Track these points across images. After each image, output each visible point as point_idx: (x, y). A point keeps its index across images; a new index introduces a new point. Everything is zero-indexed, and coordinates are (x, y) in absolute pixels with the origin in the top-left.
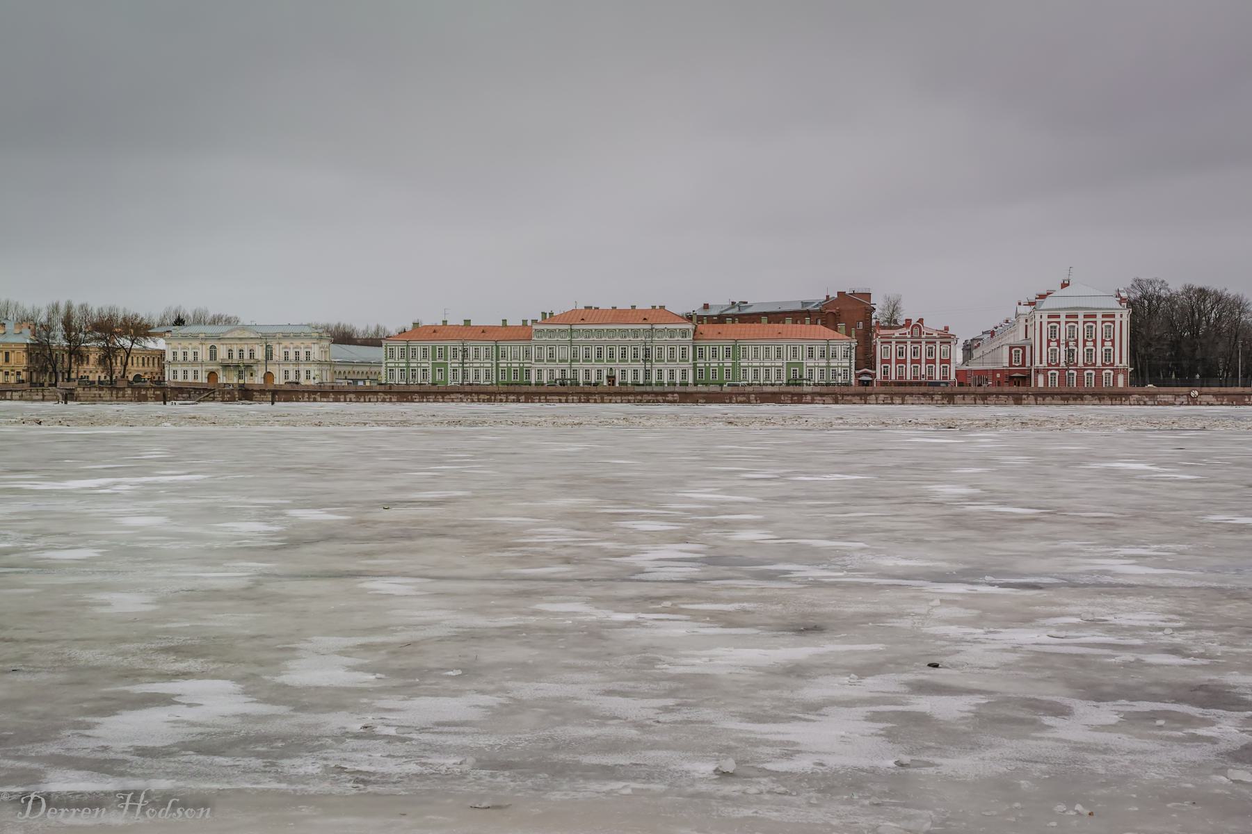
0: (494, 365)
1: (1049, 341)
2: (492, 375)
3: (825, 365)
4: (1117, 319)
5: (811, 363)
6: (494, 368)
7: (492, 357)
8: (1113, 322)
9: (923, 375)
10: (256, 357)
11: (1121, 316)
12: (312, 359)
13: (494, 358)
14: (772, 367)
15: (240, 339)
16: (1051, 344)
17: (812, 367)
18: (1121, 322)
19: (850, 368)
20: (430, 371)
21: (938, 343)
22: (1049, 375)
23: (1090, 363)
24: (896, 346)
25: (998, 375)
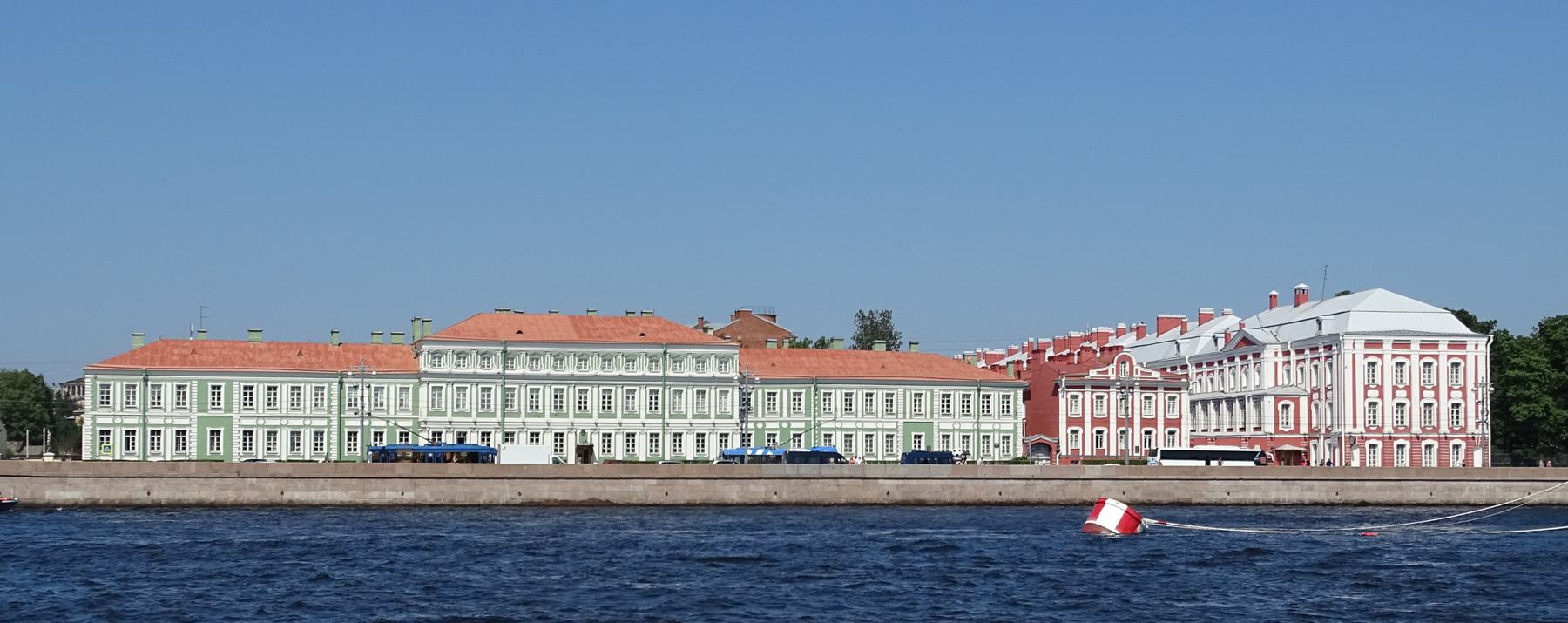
0: (335, 423)
1: (1367, 388)
2: (329, 444)
3: (970, 426)
5: (946, 424)
6: (335, 429)
7: (330, 406)
8: (1464, 357)
9: (1137, 448)
13: (335, 410)
14: (877, 429)
16: (1370, 393)
17: (950, 430)
19: (1016, 434)
20: (194, 434)
22: (1451, 447)
23: (1402, 427)
24: (1092, 393)
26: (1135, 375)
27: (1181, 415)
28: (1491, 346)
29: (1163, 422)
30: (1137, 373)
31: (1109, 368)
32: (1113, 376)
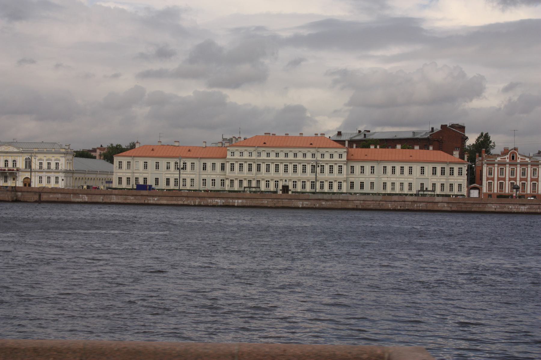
10: (18, 166)
12: (60, 168)
15: (7, 153)
24: (498, 167)
26: (518, 160)
27: (538, 176)
29: (508, 180)
30: (519, 159)
31: (506, 157)
32: (508, 160)
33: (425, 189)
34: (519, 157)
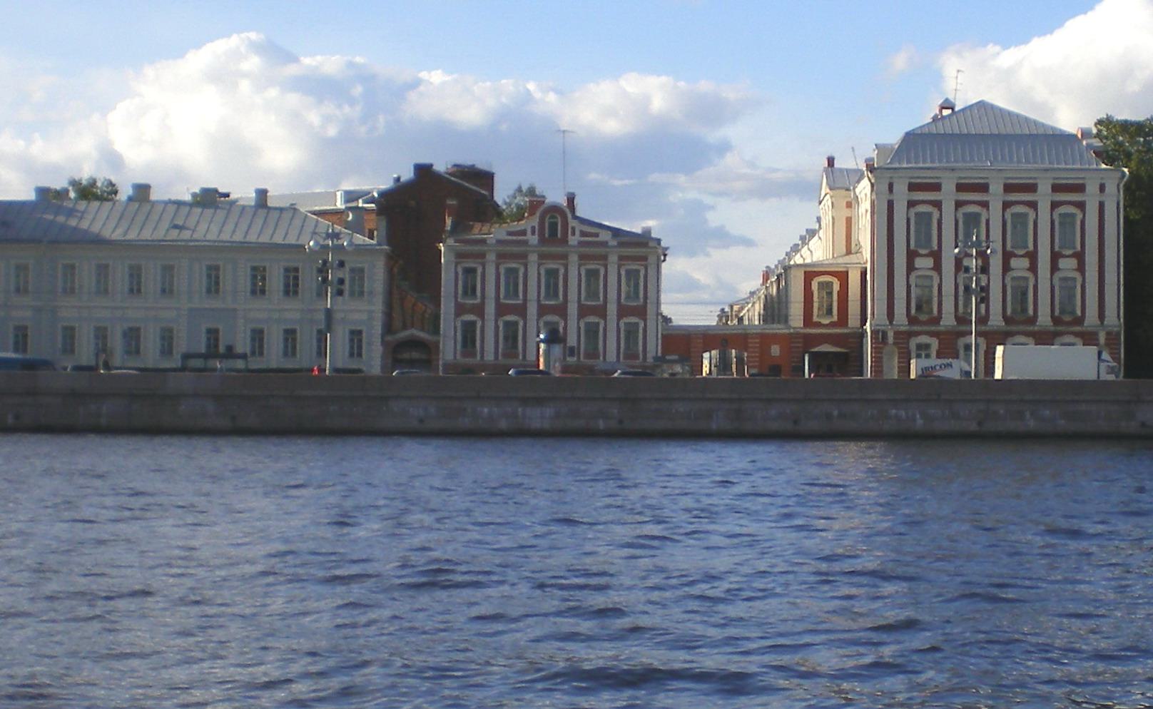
1: (911, 255)
4: (1091, 198)
8: (1081, 206)
11: (1102, 188)
18: (1102, 205)
21: (613, 259)
25: (775, 350)
28: (1125, 186)
30: (573, 234)
33: (222, 349)
34: (573, 229)
